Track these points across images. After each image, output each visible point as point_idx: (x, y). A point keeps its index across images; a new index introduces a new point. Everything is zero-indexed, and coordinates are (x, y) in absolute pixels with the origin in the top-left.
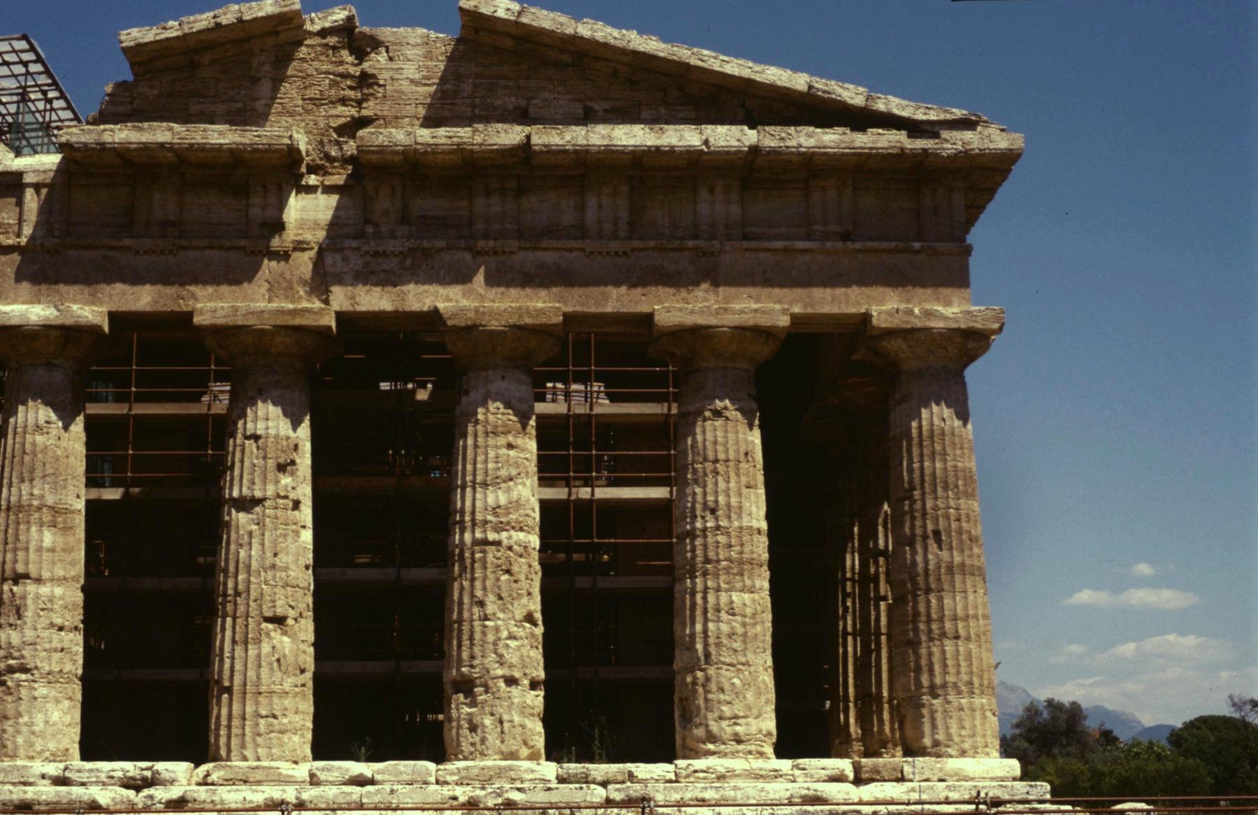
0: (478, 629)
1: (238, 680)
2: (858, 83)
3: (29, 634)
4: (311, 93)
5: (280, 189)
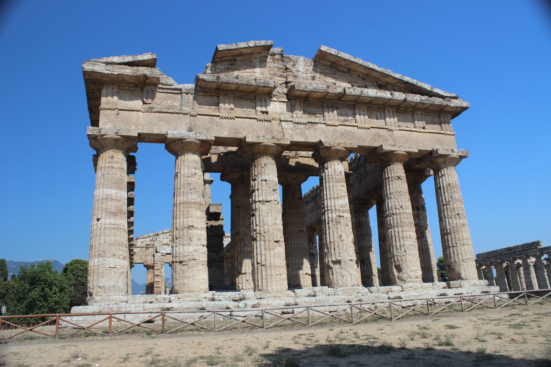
0: (340, 244)
1: (268, 262)
2: (429, 84)
3: (196, 248)
4: (272, 72)
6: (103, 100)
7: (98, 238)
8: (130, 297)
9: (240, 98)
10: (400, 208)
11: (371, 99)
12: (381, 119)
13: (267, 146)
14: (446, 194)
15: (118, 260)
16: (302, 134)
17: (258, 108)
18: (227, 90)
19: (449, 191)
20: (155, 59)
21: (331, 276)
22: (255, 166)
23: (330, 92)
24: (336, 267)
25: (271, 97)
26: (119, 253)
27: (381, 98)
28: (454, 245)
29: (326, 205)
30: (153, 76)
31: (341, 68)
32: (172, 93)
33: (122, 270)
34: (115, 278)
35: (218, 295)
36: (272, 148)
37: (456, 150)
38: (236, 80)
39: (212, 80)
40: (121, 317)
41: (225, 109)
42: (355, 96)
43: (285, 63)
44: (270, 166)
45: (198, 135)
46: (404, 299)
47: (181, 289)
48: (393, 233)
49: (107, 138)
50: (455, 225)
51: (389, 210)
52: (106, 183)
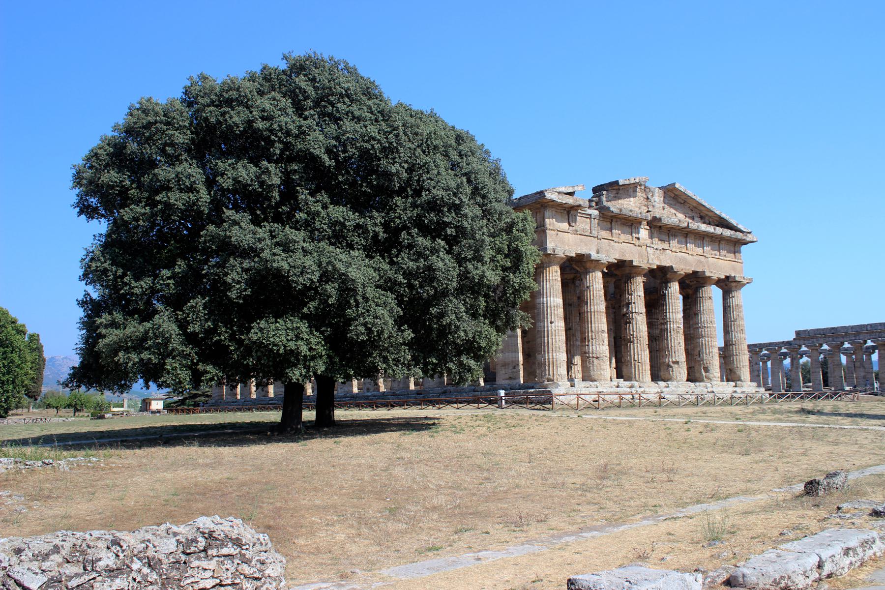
6: (547, 221)
16: (658, 258)
24: (675, 366)
31: (680, 200)
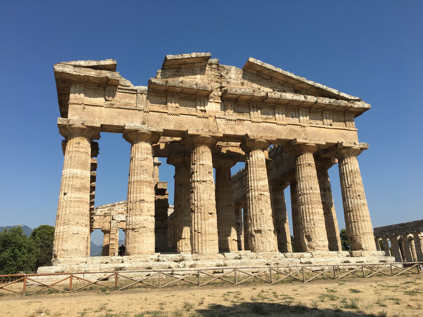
0: (261, 217)
1: (203, 230)
2: (336, 89)
3: (146, 218)
4: (209, 79)
5: (204, 101)
6: (72, 96)
7: (64, 209)
8: (89, 259)
9: (184, 98)
10: (310, 189)
11: (288, 101)
12: (296, 117)
13: (204, 138)
14: (349, 179)
15: (81, 227)
16: (232, 128)
17: (198, 107)
18: (174, 92)
19: (351, 176)
20: (116, 65)
21: (253, 242)
22: (195, 153)
23: (256, 95)
24: (257, 236)
25: (209, 99)
26: (81, 222)
27: (296, 100)
28: (356, 220)
29: (250, 185)
30: (113, 78)
31: (265, 76)
32: (130, 93)
33: (84, 236)
34: (77, 242)
35: (163, 257)
36: (209, 139)
37: (357, 143)
38: (181, 84)
39: (162, 84)
40: (80, 276)
41: (172, 107)
42: (276, 98)
43: (220, 72)
44: (207, 153)
45: (150, 127)
46: (315, 264)
47: (132, 252)
48: (304, 209)
49: (75, 127)
50: (356, 204)
51: (301, 190)
52: (73, 164)
